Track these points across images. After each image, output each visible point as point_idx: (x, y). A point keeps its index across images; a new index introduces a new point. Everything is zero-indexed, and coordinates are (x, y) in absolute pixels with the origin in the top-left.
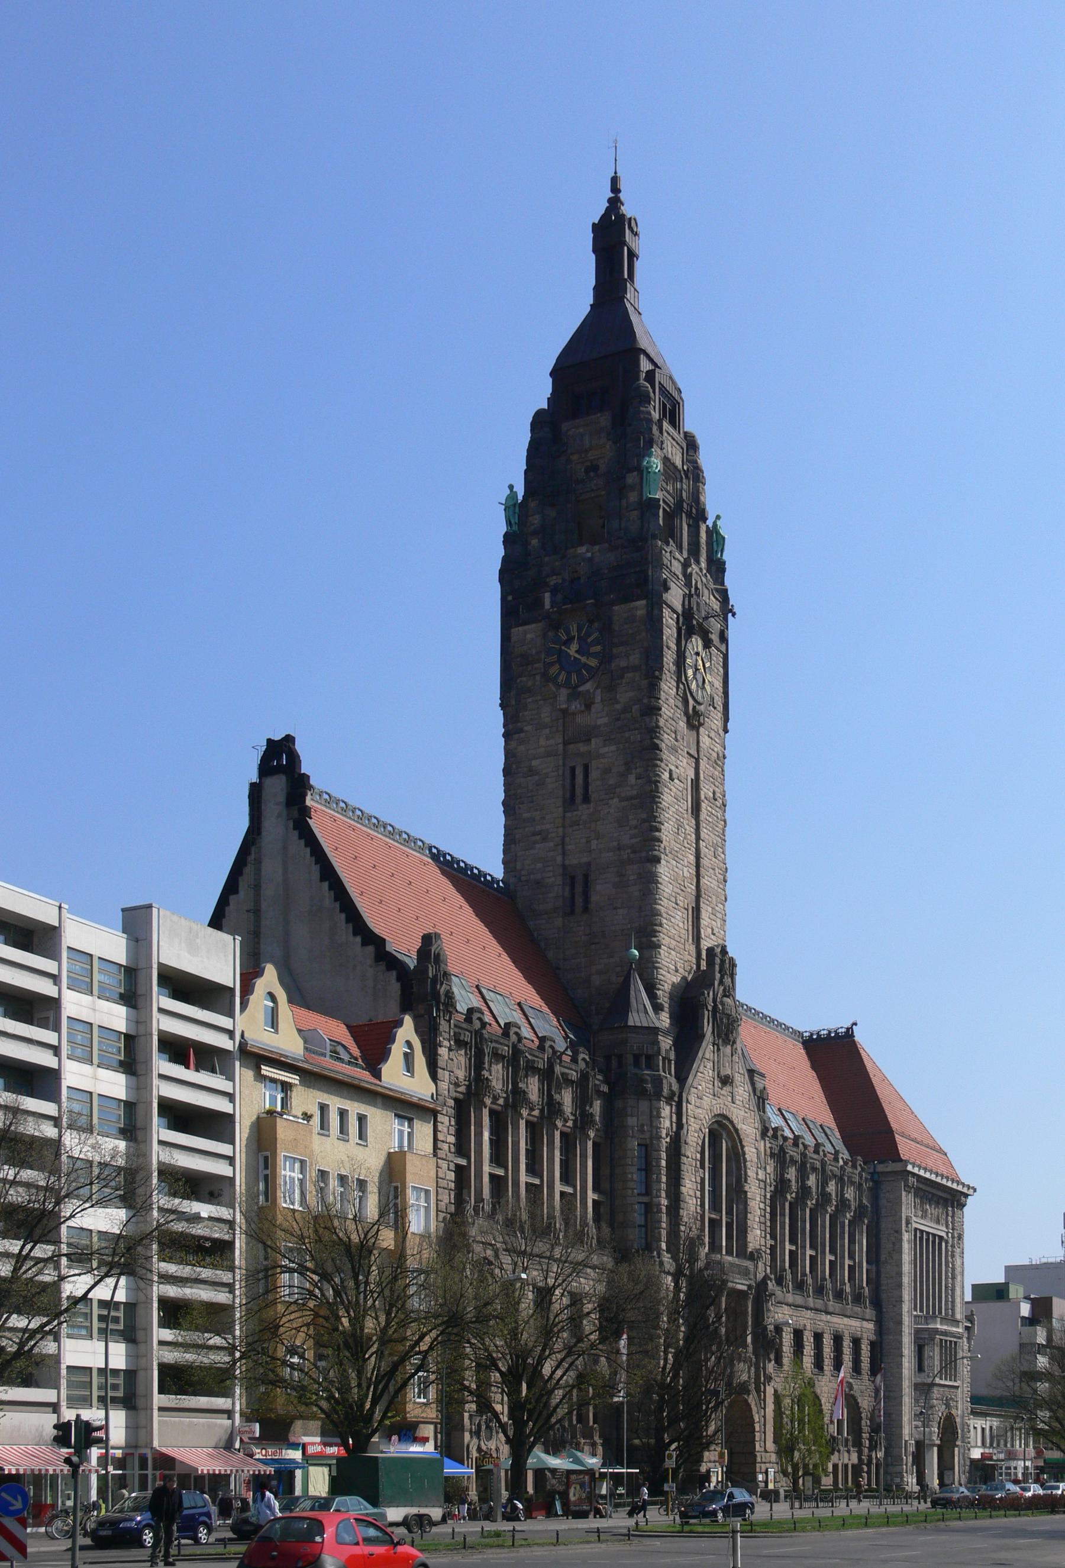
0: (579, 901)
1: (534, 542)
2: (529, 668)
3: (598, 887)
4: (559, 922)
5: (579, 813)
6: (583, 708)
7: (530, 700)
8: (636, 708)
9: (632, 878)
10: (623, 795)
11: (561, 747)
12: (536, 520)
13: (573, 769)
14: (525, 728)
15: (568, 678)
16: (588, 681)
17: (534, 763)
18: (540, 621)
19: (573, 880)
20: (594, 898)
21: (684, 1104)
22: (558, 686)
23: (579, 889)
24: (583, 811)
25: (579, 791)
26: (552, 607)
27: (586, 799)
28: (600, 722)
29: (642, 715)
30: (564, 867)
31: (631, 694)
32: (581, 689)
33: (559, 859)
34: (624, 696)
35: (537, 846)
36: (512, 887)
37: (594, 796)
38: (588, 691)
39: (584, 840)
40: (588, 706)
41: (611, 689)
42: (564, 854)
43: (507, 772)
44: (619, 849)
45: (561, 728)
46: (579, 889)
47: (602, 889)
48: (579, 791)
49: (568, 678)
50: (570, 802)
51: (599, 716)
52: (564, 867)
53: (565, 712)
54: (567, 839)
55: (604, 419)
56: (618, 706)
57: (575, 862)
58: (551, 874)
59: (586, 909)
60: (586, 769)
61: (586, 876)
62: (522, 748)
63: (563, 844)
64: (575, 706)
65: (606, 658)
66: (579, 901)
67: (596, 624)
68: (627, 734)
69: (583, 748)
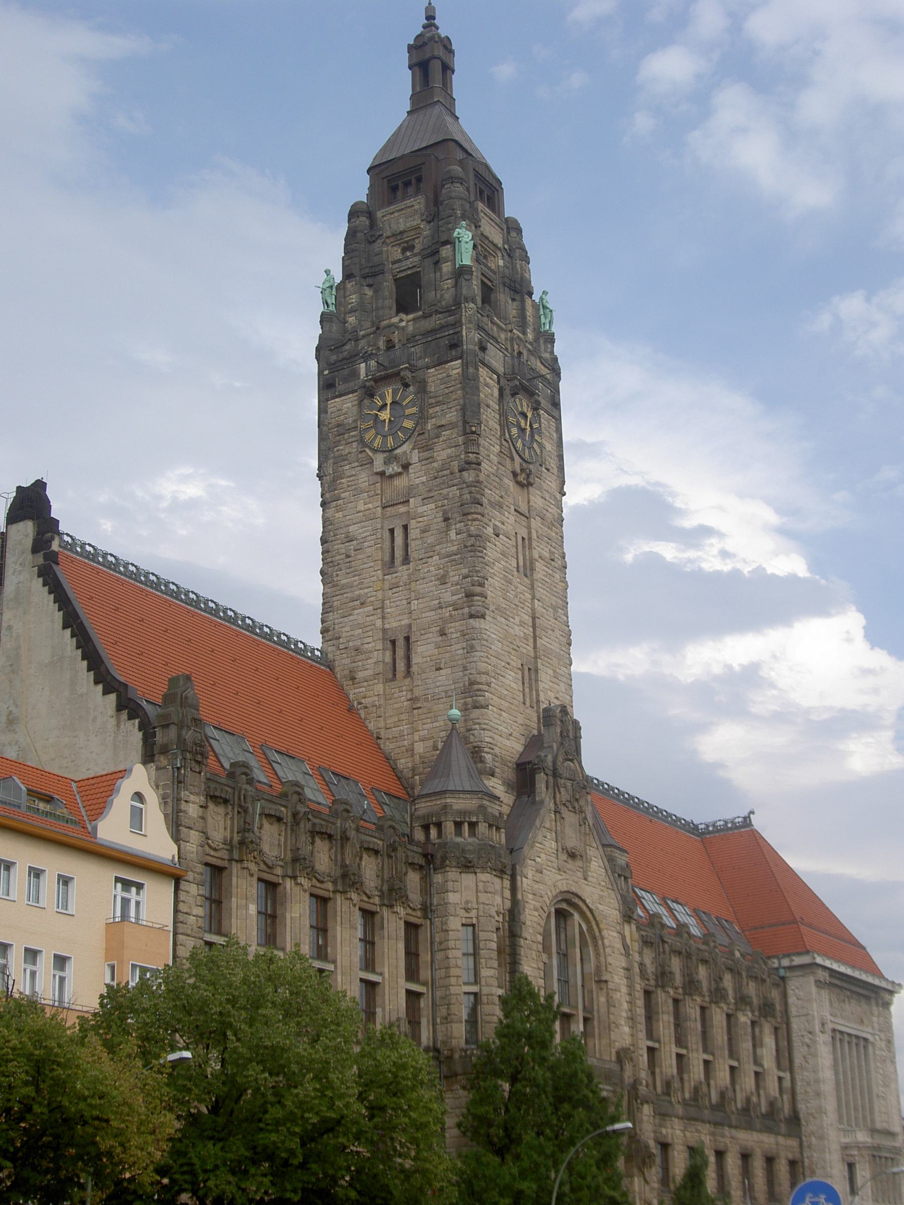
0: (401, 666)
1: (351, 319)
2: (346, 436)
3: (420, 649)
4: (379, 688)
5: (399, 574)
6: (400, 470)
7: (347, 467)
8: (455, 465)
9: (454, 636)
10: (443, 551)
11: (379, 509)
12: (354, 299)
13: (392, 531)
14: (343, 495)
15: (384, 442)
16: (404, 442)
17: (351, 528)
18: (355, 391)
19: (393, 642)
20: (416, 659)
21: (519, 878)
22: (375, 451)
23: (400, 652)
24: (403, 573)
25: (399, 553)
26: (367, 375)
27: (406, 560)
28: (417, 481)
29: (460, 471)
30: (384, 631)
31: (449, 451)
32: (398, 451)
33: (379, 623)
34: (442, 454)
35: (356, 612)
36: (330, 656)
37: (413, 555)
38: (405, 453)
39: (405, 602)
40: (406, 467)
41: (427, 448)
42: (383, 618)
43: (324, 541)
44: (441, 608)
45: (379, 492)
46: (400, 652)
47: (423, 652)
48: (399, 553)
49: (384, 442)
50: (390, 564)
51: (417, 476)
52: (384, 631)
53: (382, 474)
54: (387, 602)
55: (418, 203)
56: (435, 465)
57: (395, 625)
58: (370, 640)
59: (408, 673)
60: (405, 528)
61: (407, 639)
62: (340, 514)
63: (383, 608)
64: (394, 468)
65: (422, 417)
66: (401, 666)
67: (411, 388)
68: (445, 491)
69: (402, 509)
